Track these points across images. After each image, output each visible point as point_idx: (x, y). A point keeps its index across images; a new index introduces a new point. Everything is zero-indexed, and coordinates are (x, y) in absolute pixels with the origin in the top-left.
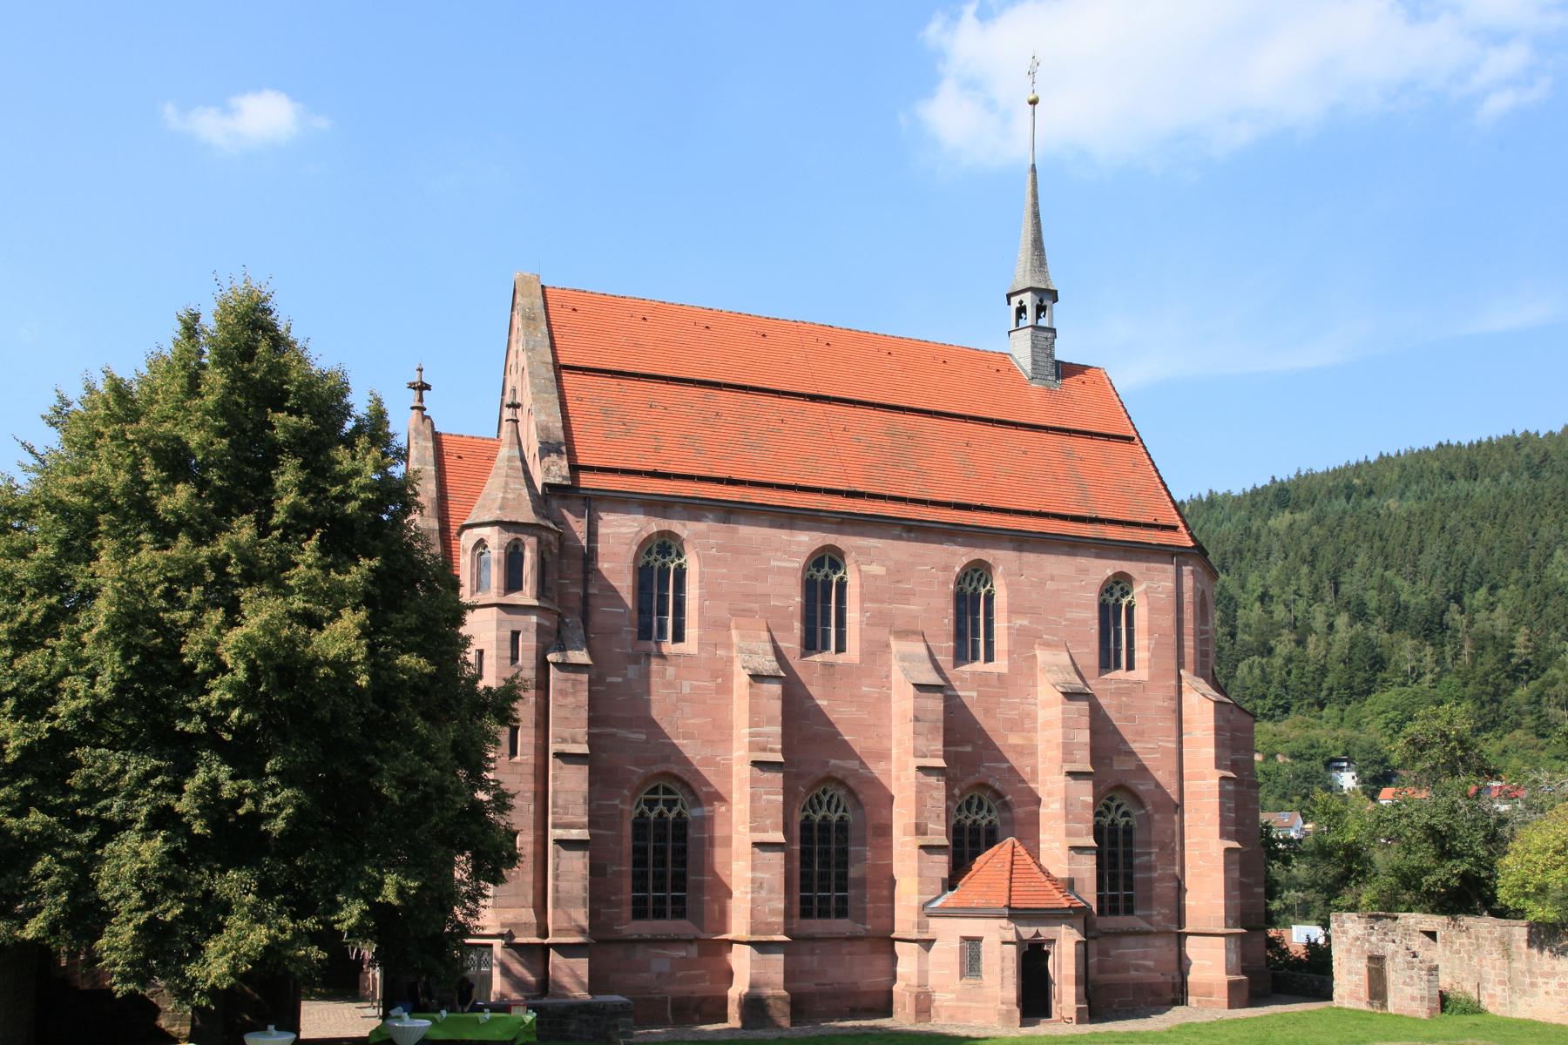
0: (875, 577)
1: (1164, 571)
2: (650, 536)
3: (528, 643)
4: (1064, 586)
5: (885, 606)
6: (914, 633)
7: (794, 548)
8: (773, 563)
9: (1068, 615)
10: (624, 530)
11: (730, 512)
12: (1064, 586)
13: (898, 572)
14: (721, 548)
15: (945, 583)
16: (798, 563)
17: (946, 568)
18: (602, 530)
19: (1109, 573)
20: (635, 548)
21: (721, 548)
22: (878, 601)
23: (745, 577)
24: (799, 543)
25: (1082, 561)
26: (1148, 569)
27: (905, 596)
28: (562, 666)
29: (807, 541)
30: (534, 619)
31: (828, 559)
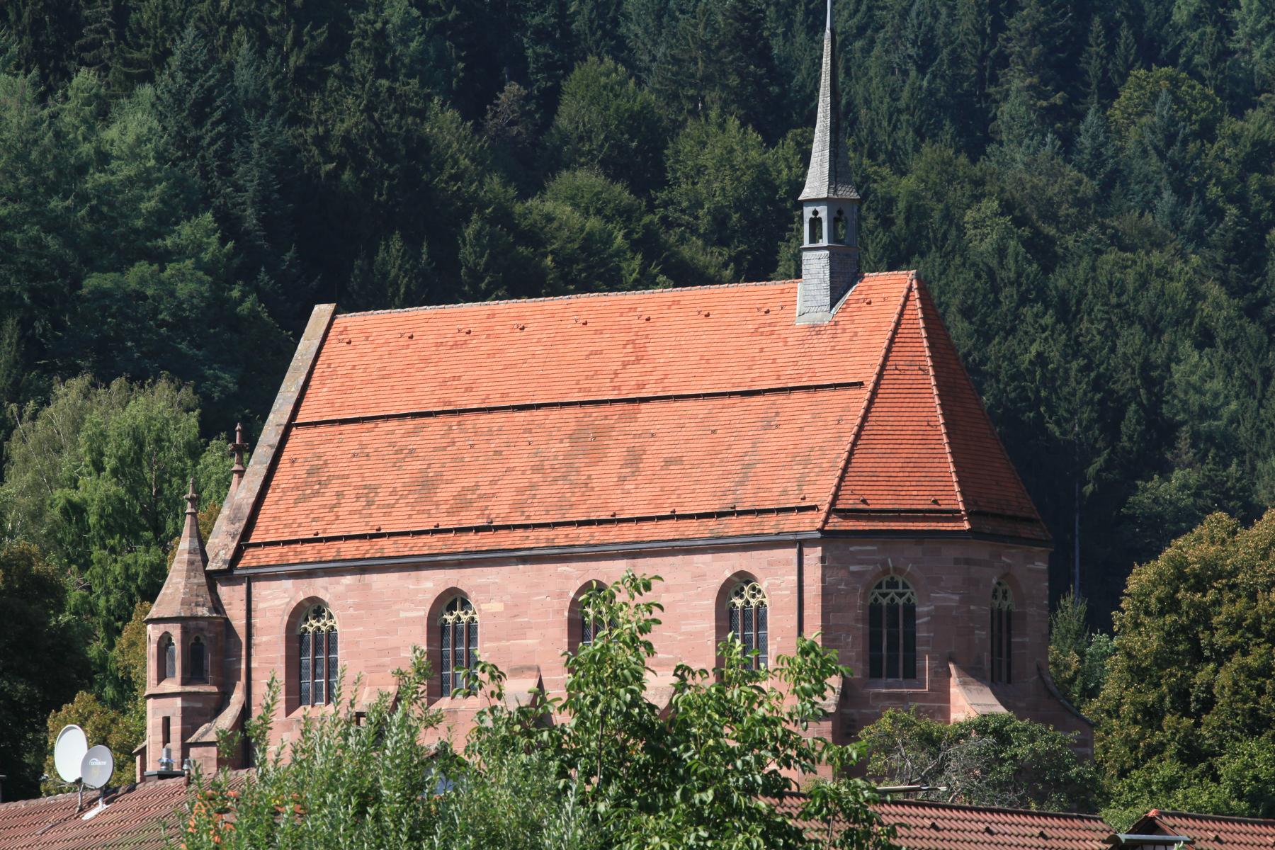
0: (494, 615)
1: (787, 563)
2: (300, 605)
3: (176, 727)
4: (679, 596)
5: (504, 643)
6: (530, 668)
7: (420, 597)
8: (403, 615)
9: (684, 629)
10: (277, 602)
11: (363, 567)
12: (679, 596)
13: (515, 608)
14: (357, 607)
15: (559, 612)
16: (423, 612)
17: (561, 595)
18: (259, 605)
19: (728, 574)
20: (286, 618)
21: (357, 607)
22: (498, 639)
23: (379, 632)
24: (425, 591)
25: (701, 561)
26: (770, 564)
27: (521, 631)
28: (197, 744)
29: (433, 583)
30: (178, 702)
31: (453, 599)
